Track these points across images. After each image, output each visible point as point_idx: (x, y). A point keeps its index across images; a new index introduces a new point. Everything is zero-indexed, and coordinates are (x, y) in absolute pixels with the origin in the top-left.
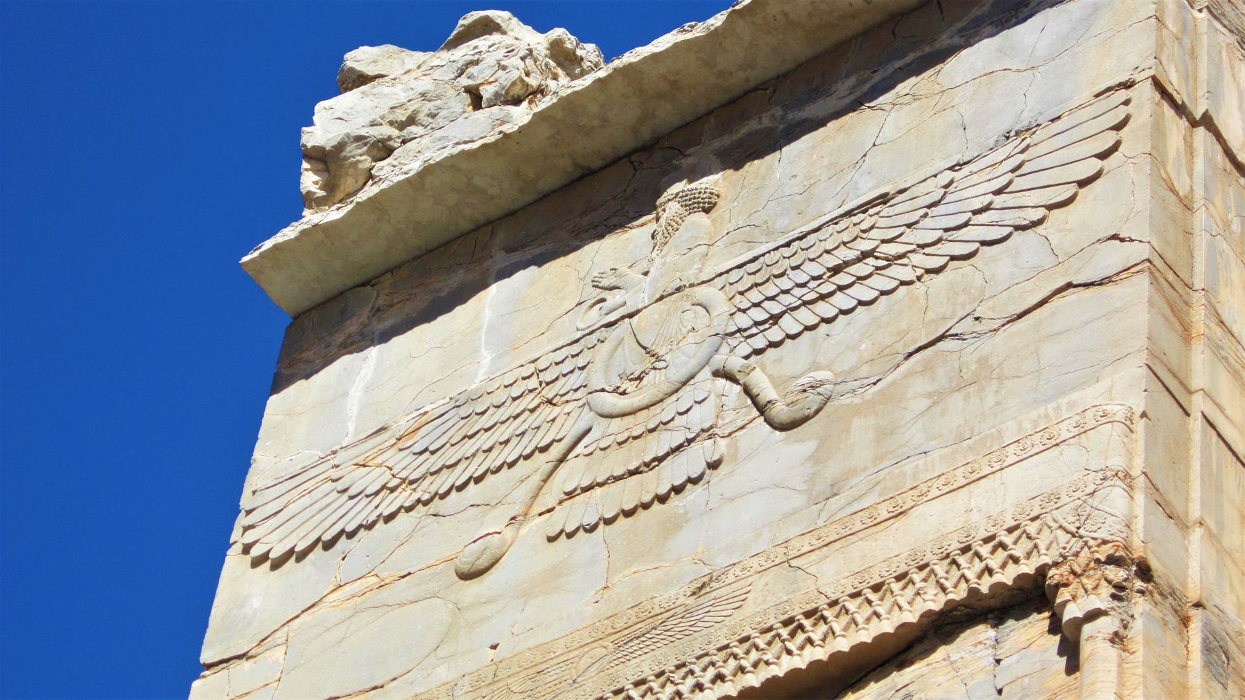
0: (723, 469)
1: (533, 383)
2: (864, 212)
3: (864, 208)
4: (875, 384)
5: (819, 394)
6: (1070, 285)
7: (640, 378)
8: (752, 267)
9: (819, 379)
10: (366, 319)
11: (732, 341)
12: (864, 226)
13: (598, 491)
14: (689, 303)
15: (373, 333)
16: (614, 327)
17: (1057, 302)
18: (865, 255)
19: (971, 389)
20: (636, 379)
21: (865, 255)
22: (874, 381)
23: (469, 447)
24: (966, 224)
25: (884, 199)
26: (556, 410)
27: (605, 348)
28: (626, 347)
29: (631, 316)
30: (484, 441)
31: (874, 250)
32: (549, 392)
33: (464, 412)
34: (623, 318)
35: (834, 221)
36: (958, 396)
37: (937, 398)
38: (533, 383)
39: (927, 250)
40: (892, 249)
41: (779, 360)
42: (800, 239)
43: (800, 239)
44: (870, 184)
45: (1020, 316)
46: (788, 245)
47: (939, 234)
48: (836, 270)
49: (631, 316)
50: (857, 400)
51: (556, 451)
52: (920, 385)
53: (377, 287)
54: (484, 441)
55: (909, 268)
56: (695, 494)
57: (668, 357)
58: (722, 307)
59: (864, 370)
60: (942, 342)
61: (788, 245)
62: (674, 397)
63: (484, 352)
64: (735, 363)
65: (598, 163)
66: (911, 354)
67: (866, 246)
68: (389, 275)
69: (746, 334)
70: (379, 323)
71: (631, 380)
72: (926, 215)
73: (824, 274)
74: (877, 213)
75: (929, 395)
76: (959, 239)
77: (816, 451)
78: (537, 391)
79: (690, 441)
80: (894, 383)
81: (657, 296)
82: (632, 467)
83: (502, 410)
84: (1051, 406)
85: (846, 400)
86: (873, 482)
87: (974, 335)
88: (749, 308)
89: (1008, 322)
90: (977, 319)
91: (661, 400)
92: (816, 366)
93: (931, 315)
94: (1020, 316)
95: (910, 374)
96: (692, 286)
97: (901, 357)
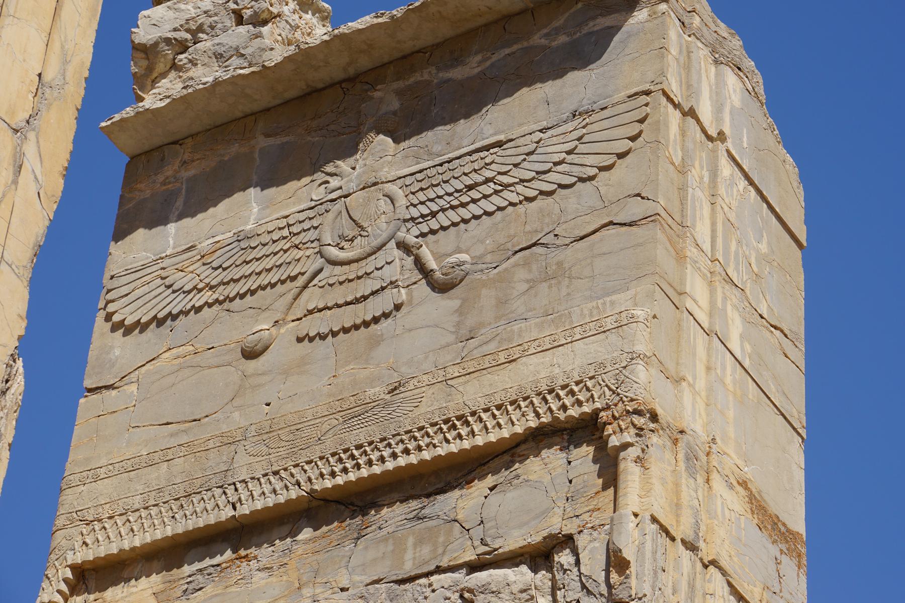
0: (404, 310)
1: (285, 232)
2: (488, 151)
3: (487, 148)
4: (495, 268)
5: (462, 270)
6: (611, 223)
7: (352, 240)
8: (419, 176)
9: (462, 260)
10: (177, 168)
11: (409, 225)
12: (488, 160)
13: (328, 313)
14: (381, 194)
15: (182, 178)
16: (335, 202)
17: (604, 232)
18: (488, 180)
19: (553, 282)
20: (349, 241)
21: (488, 180)
22: (495, 266)
23: (247, 270)
24: (549, 171)
25: (499, 144)
26: (301, 253)
27: (330, 216)
28: (343, 217)
29: (346, 196)
30: (256, 267)
31: (494, 178)
32: (296, 240)
33: (244, 244)
34: (340, 197)
35: (470, 154)
36: (545, 285)
37: (533, 284)
38: (285, 232)
39: (525, 184)
40: (505, 179)
41: (436, 242)
42: (449, 162)
43: (449, 162)
44: (491, 132)
45: (582, 238)
46: (441, 165)
47: (534, 174)
48: (470, 188)
49: (346, 196)
50: (484, 277)
51: (301, 281)
52: (521, 274)
53: (183, 146)
54: (256, 267)
55: (515, 193)
56: (387, 323)
57: (369, 229)
58: (402, 202)
59: (489, 258)
60: (535, 248)
61: (441, 165)
62: (373, 257)
63: (254, 205)
64: (411, 239)
65: (321, 85)
66: (516, 252)
67: (489, 174)
68: (190, 140)
69: (416, 221)
70: (185, 171)
71: (346, 241)
72: (525, 160)
73: (463, 189)
74: (495, 153)
75: (528, 281)
76: (545, 179)
77: (460, 306)
78: (289, 238)
79: (383, 288)
80: (506, 270)
81: (362, 186)
82: (348, 300)
83: (266, 247)
84: (600, 301)
85: (478, 276)
86: (495, 333)
87: (555, 246)
88: (418, 204)
89: (575, 241)
90: (556, 235)
91: (366, 258)
92: (459, 251)
93: (528, 228)
94: (582, 238)
95: (516, 265)
96: (382, 183)
97: (510, 253)
